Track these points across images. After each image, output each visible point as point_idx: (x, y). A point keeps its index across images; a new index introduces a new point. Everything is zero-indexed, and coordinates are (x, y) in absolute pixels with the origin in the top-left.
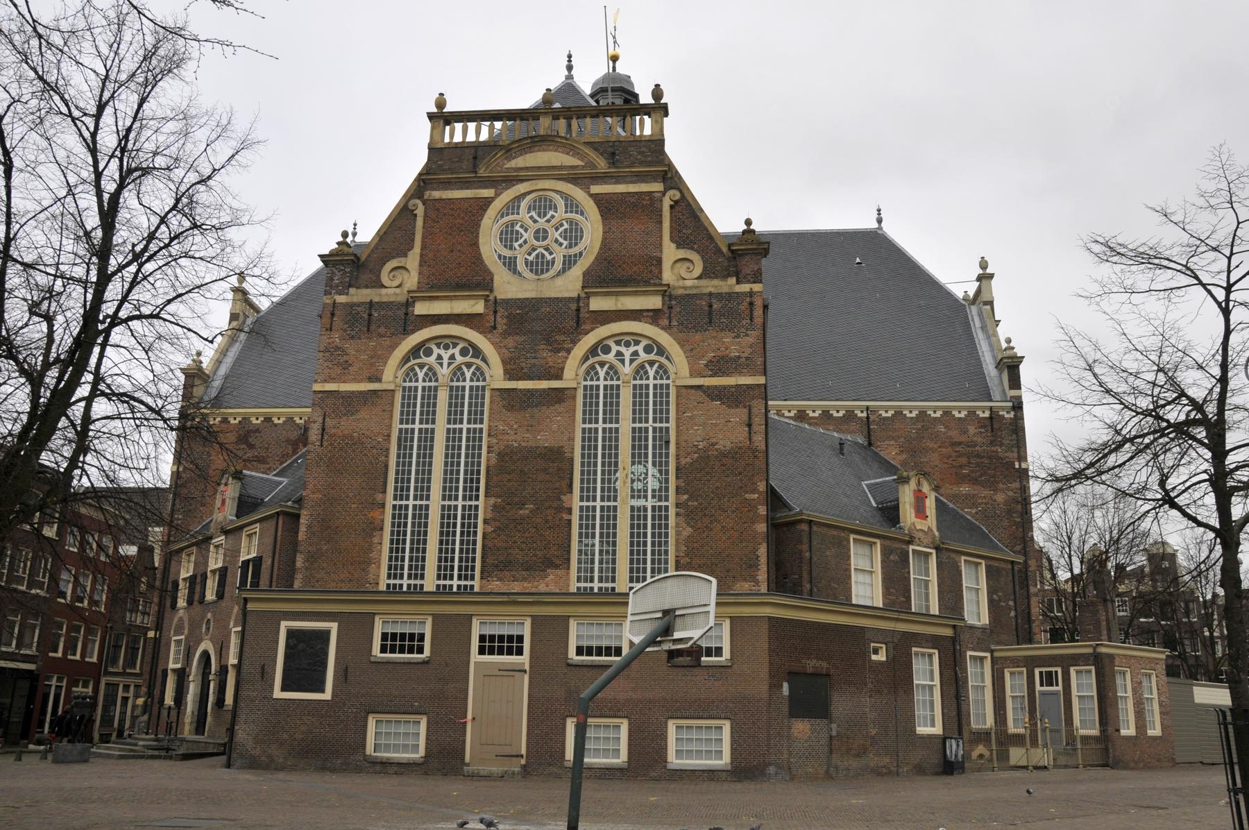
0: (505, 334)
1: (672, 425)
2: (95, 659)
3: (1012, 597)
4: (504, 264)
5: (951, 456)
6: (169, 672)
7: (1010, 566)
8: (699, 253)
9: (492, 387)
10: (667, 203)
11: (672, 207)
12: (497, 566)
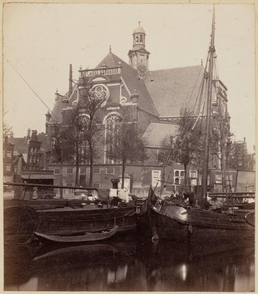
10: (121, 87)
11: (122, 88)
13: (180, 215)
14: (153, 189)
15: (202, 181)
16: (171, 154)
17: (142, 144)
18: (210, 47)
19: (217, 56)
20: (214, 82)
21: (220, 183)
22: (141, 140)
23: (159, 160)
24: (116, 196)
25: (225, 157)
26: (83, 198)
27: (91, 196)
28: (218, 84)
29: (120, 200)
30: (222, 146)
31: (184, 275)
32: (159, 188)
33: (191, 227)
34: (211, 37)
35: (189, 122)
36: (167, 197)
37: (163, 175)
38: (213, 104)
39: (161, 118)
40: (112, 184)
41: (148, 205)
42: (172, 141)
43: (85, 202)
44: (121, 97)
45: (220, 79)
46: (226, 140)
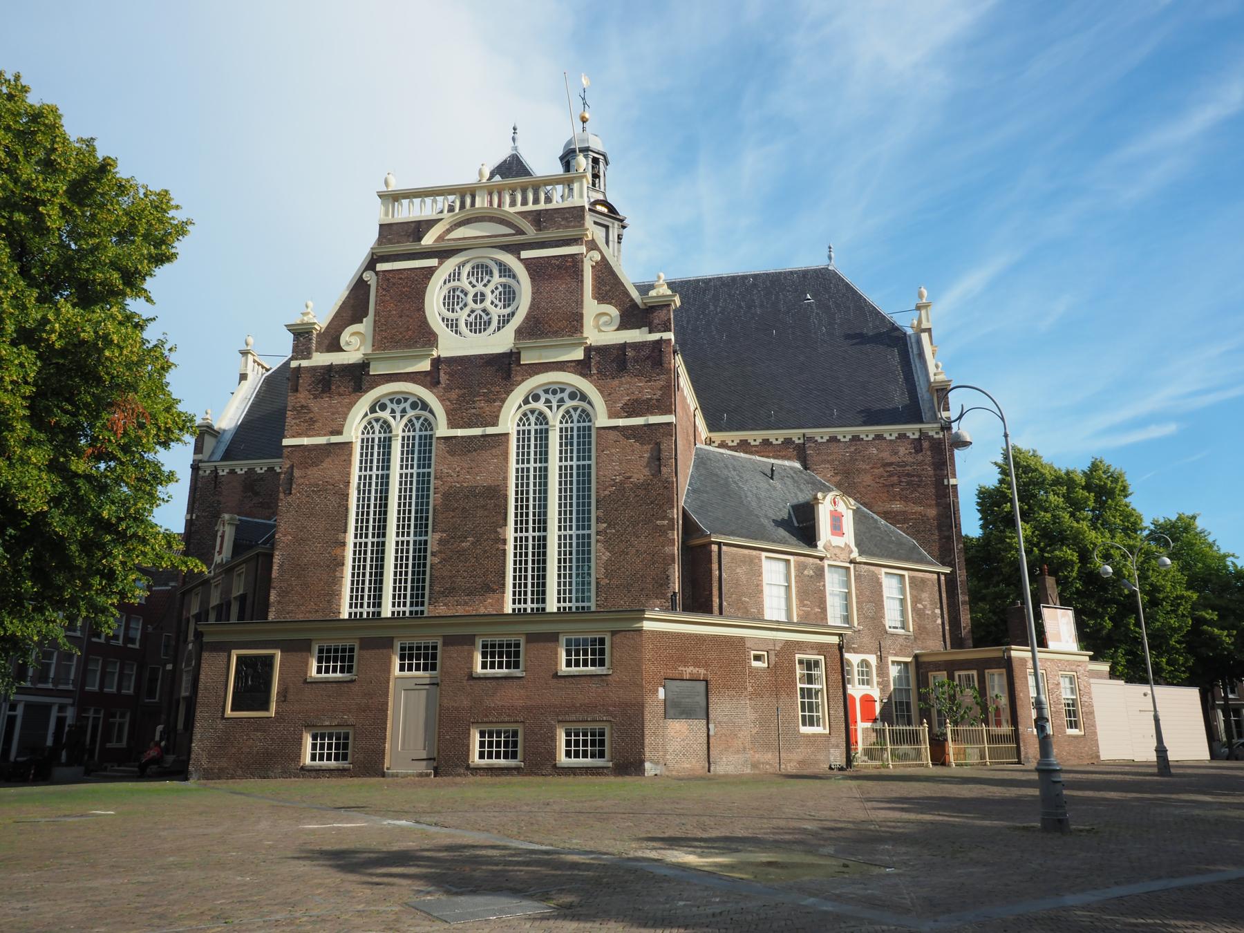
0: (448, 389)
1: (593, 462)
2: (131, 691)
3: (938, 606)
4: (447, 326)
5: (882, 476)
6: (181, 700)
7: (935, 576)
8: (616, 306)
9: (437, 436)
12: (443, 593)
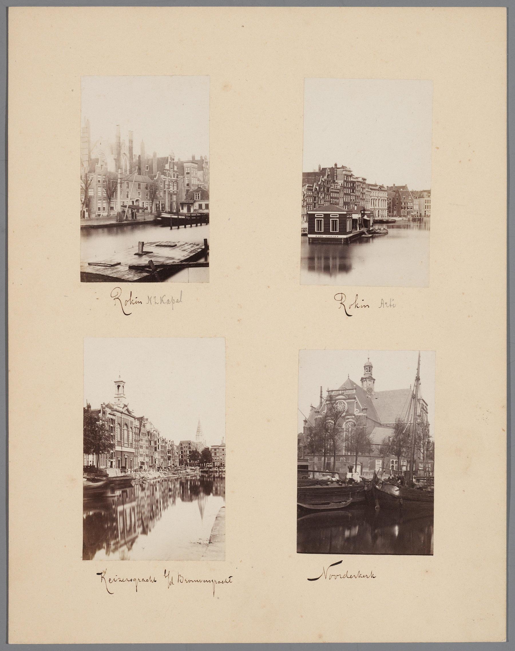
13: (394, 492)
14: (376, 473)
15: (410, 467)
16: (389, 449)
17: (369, 441)
18: (416, 377)
19: (421, 383)
20: (419, 400)
21: (422, 469)
22: (369, 439)
23: (380, 453)
24: (351, 477)
25: (426, 451)
26: (328, 478)
27: (334, 477)
28: (421, 402)
29: (354, 480)
30: (424, 444)
31: (397, 533)
32: (380, 472)
33: (402, 499)
34: (417, 370)
35: (401, 428)
36: (386, 479)
37: (383, 463)
38: (418, 415)
39: (382, 424)
40: (348, 469)
41: (373, 484)
42: (389, 440)
43: (329, 481)
44: (356, 409)
45: (422, 398)
46: (427, 440)
